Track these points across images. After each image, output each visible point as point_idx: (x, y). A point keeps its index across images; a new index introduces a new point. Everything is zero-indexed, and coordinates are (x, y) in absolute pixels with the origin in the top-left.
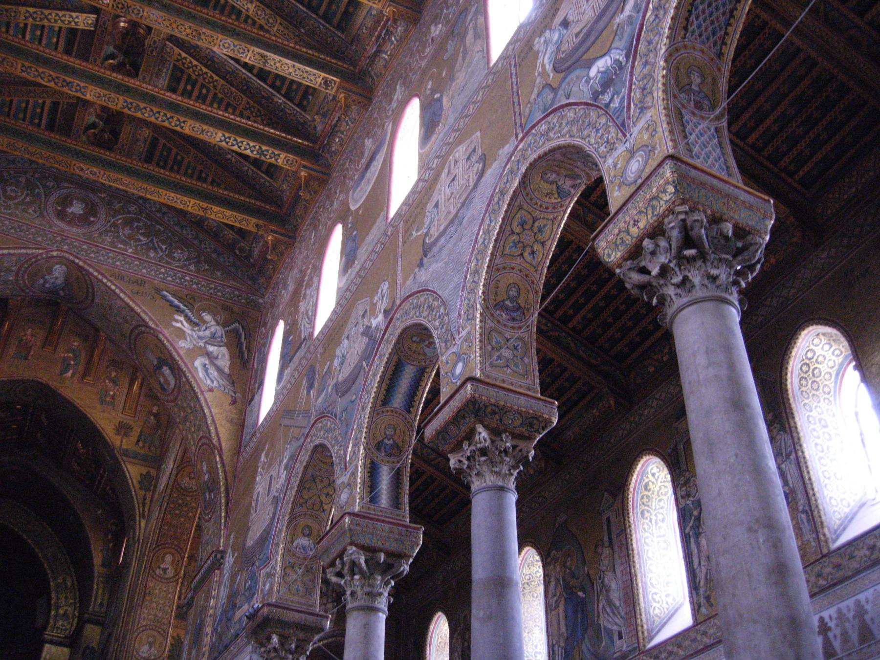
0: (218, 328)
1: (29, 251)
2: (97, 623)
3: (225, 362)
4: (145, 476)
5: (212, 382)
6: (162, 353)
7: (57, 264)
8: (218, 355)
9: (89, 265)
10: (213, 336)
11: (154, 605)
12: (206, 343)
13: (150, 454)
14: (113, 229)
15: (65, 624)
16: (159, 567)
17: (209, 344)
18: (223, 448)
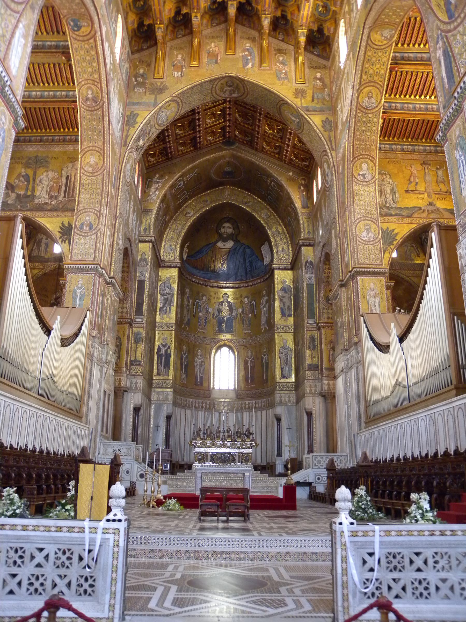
2: (310, 245)
4: (325, 122)
11: (362, 202)
13: (324, 106)
16: (359, 175)
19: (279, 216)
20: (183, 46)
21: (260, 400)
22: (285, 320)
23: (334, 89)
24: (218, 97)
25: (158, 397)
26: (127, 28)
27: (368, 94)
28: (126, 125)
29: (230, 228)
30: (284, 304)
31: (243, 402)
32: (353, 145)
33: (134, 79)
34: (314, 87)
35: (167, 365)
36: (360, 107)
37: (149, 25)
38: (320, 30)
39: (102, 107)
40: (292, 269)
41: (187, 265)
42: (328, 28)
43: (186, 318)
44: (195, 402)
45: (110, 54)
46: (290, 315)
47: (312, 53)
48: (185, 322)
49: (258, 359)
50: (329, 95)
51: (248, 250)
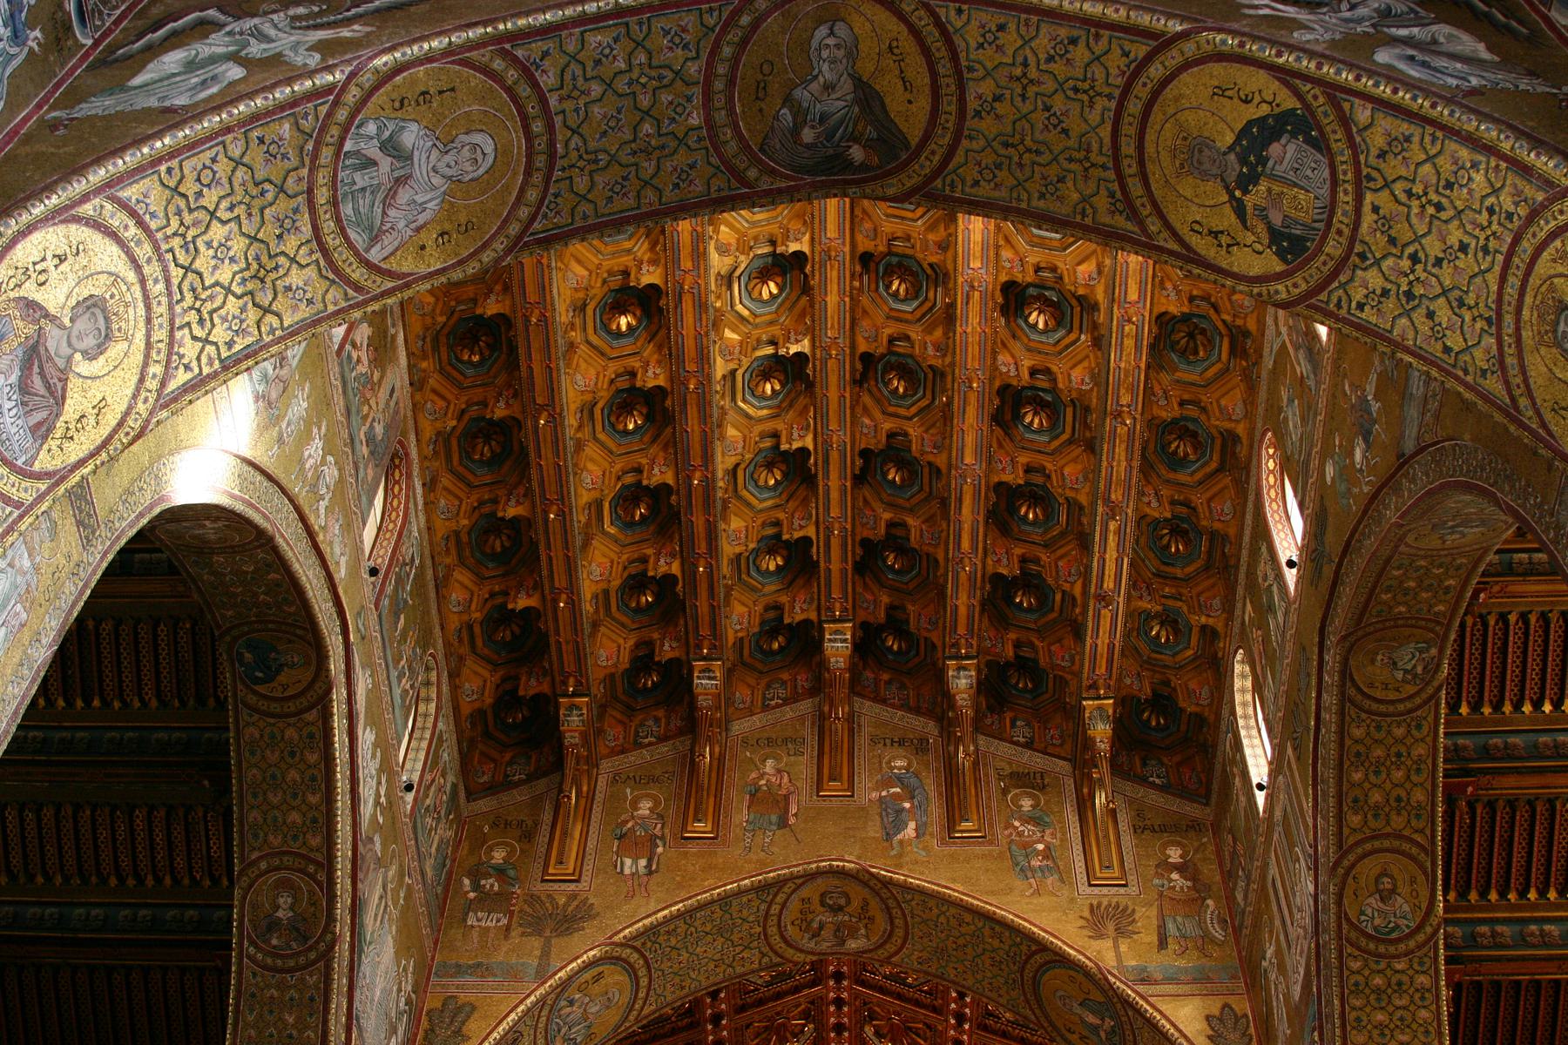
20: (658, 772)
23: (1239, 897)
24: (790, 953)
26: (456, 709)
27: (1377, 880)
33: (467, 882)
34: (1161, 895)
36: (1353, 935)
37: (537, 697)
38: (1162, 701)
39: (327, 956)
42: (1191, 693)
45: (380, 770)
47: (1143, 781)
50: (1222, 922)
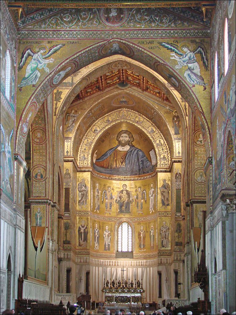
0: (191, 53)
1: (101, 43)
2: (179, 162)
3: (197, 71)
5: (194, 82)
6: (169, 73)
7: (114, 43)
8: (194, 68)
9: (127, 41)
10: (190, 58)
11: (199, 158)
12: (187, 63)
14: (132, 18)
15: (165, 162)
16: (198, 141)
17: (189, 63)
18: (204, 112)
19: (161, 132)
21: (149, 260)
22: (164, 208)
25: (81, 261)
28: (55, 100)
29: (127, 137)
30: (164, 197)
31: (138, 261)
32: (194, 124)
35: (86, 239)
40: (170, 172)
41: (96, 166)
43: (97, 204)
44: (105, 262)
46: (168, 205)
48: (96, 208)
49: (147, 232)
51: (140, 153)
